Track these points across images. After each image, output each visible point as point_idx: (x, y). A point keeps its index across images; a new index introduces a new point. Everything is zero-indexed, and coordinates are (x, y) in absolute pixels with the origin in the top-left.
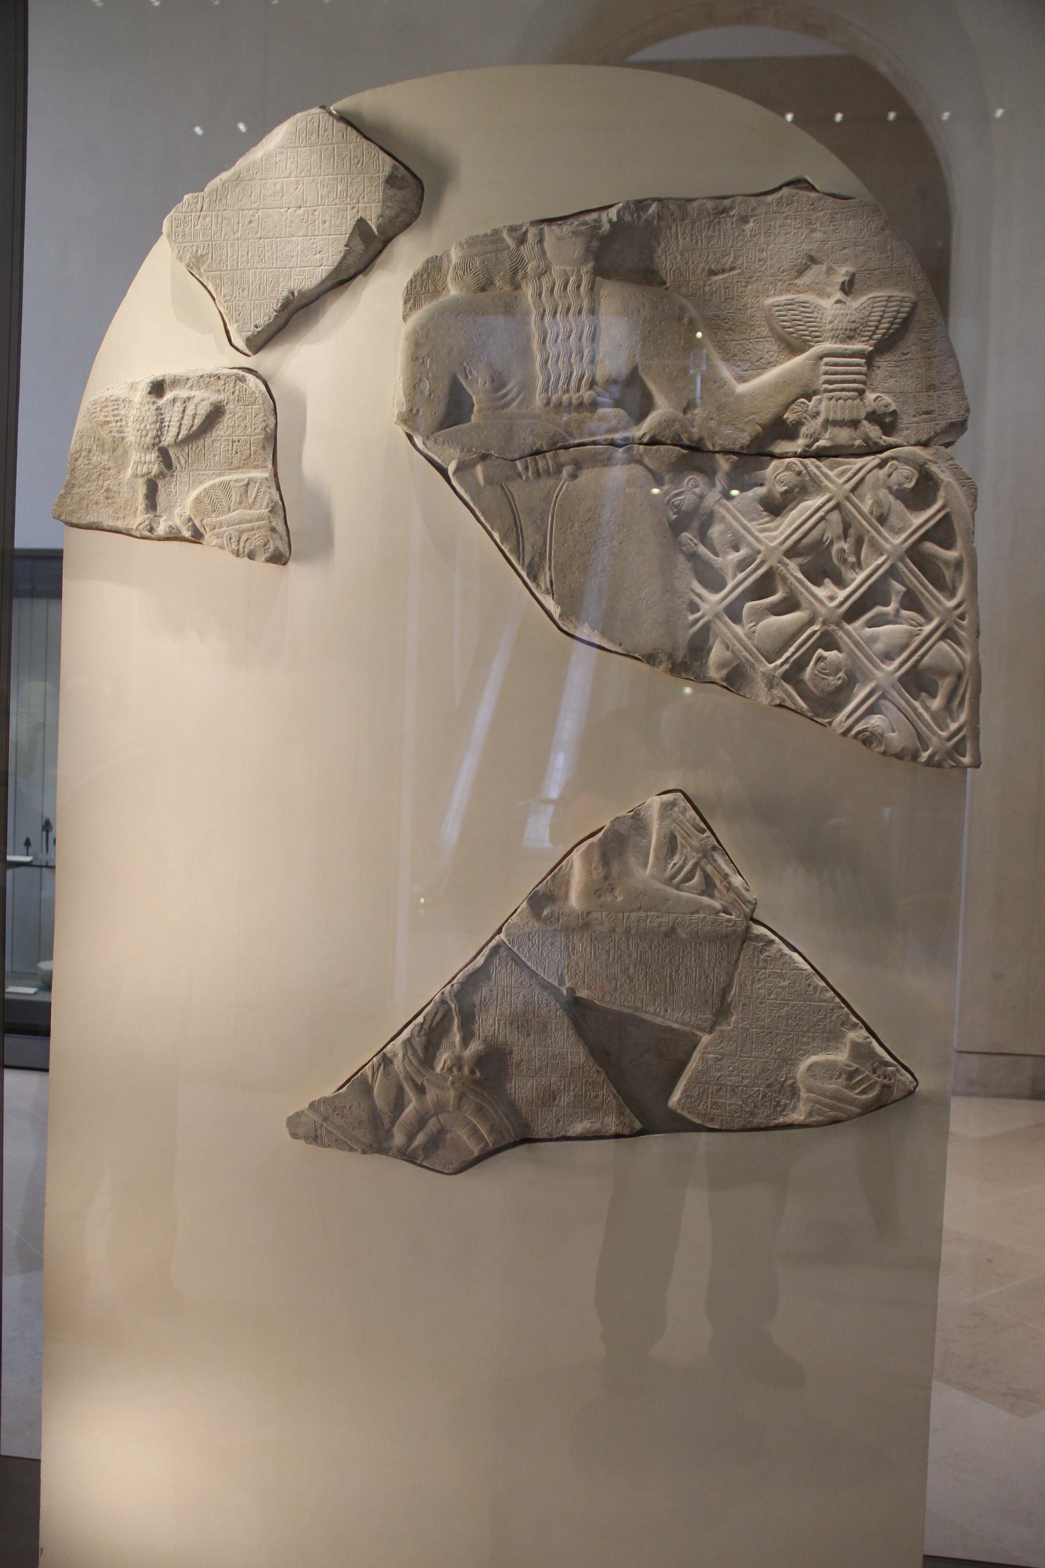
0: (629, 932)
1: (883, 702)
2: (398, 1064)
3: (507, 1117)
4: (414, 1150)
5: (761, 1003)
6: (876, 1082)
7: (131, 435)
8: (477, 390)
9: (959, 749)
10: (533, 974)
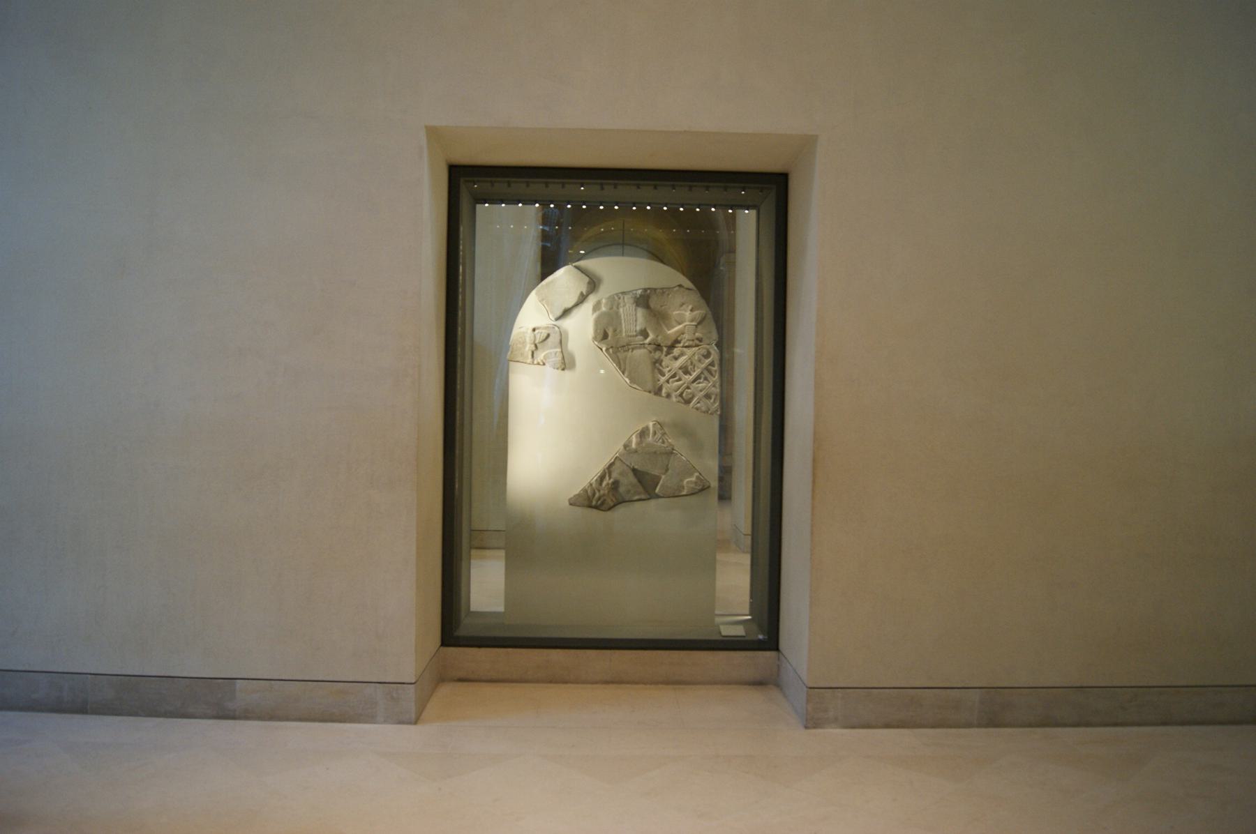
7: (528, 340)
8: (610, 333)
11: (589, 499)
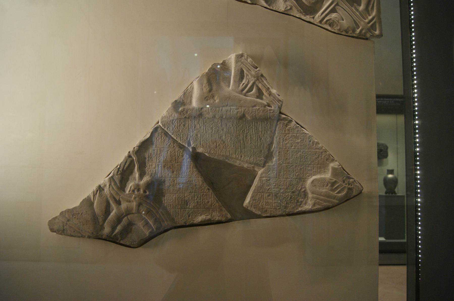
0: (222, 117)
1: (337, 7)
2: (106, 190)
3: (163, 215)
4: (115, 235)
5: (288, 151)
6: (345, 187)
9: (373, 27)
10: (175, 141)
11: (96, 222)
